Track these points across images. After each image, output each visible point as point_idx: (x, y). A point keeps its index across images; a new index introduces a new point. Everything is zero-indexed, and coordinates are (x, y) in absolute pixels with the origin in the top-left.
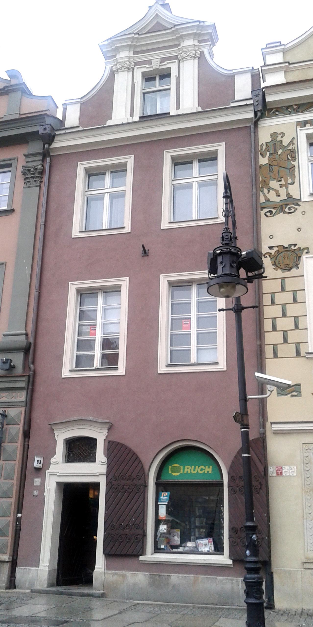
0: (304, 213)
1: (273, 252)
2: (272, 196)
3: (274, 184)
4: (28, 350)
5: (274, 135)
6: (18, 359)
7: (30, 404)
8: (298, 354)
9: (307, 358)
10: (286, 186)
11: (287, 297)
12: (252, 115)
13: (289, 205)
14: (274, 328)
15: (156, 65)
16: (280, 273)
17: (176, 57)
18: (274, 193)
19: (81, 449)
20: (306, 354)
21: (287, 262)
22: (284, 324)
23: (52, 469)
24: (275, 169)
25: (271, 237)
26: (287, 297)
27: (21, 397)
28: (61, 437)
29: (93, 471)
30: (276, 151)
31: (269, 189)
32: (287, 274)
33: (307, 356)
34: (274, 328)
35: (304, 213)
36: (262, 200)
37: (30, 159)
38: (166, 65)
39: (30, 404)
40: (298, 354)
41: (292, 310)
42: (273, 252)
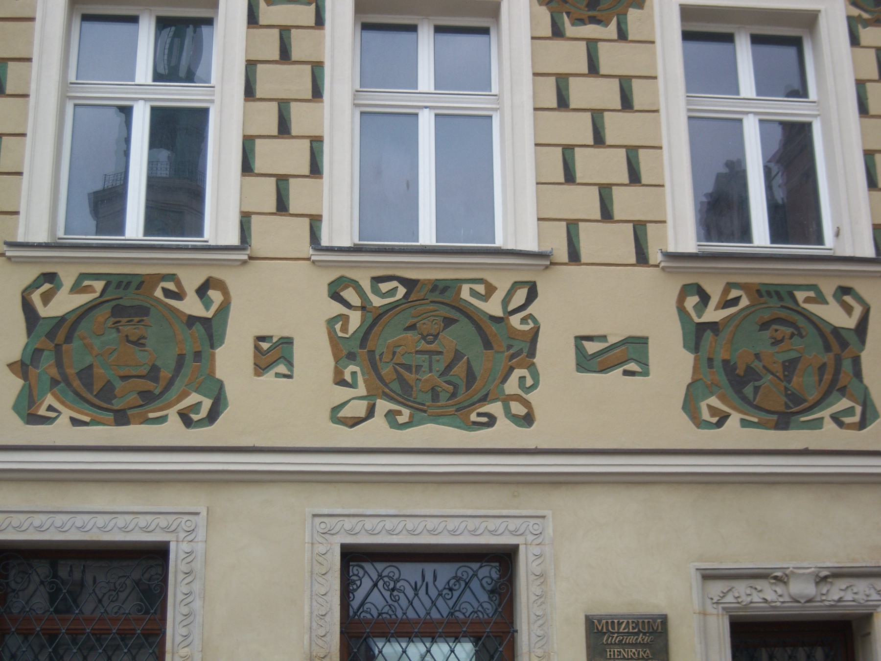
9: (9, 258)
20: (5, 248)
33: (8, 254)
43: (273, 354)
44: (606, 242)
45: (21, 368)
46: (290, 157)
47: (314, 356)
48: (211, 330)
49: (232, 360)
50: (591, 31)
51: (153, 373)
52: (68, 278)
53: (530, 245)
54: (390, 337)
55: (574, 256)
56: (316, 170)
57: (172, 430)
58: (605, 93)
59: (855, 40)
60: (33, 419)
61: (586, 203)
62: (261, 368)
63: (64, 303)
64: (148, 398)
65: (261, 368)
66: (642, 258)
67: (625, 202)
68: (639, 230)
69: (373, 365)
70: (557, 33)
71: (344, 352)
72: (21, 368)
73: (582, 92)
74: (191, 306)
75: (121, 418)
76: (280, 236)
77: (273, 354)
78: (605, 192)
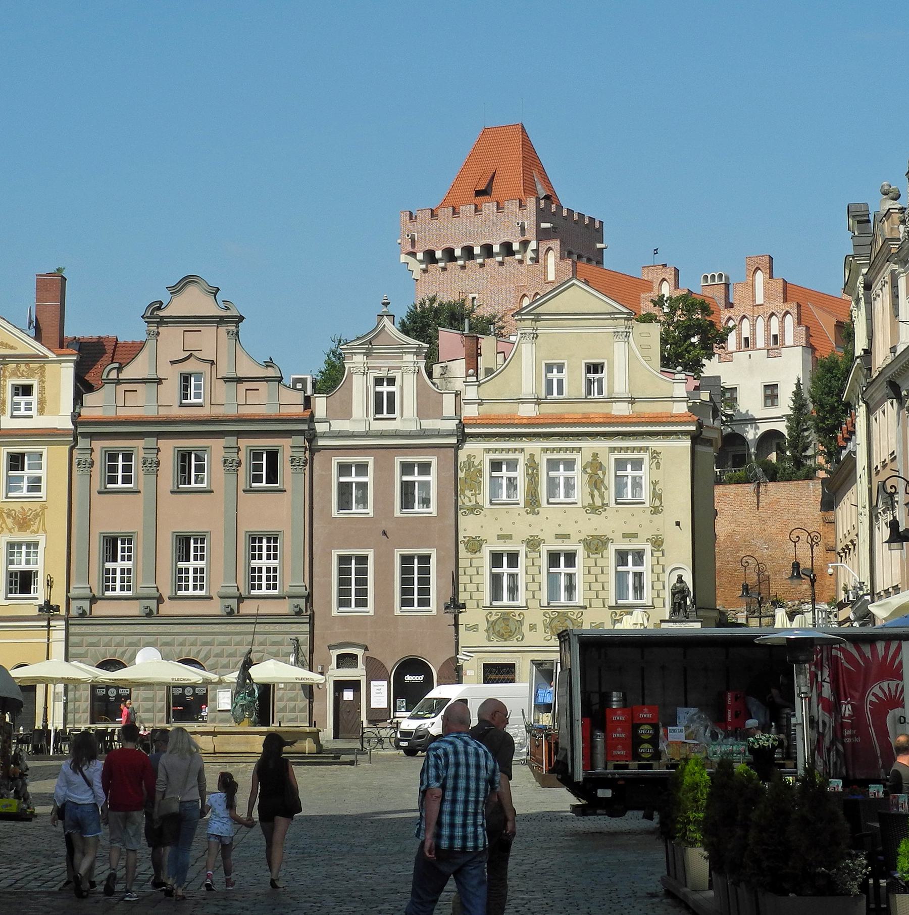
0: (485, 516)
1: (466, 540)
2: (466, 501)
3: (467, 493)
4: (309, 598)
5: (469, 456)
6: (302, 602)
7: (312, 633)
8: (478, 606)
10: (475, 495)
11: (472, 571)
12: (455, 441)
13: (476, 509)
14: (465, 590)
15: (383, 373)
16: (470, 555)
17: (400, 368)
18: (467, 499)
19: (346, 660)
21: (473, 547)
22: (471, 587)
23: (330, 672)
24: (469, 481)
25: (465, 530)
26: (472, 571)
27: (306, 628)
28: (335, 653)
29: (358, 673)
30: (469, 468)
31: (465, 495)
32: (474, 556)
34: (465, 590)
35: (485, 516)
36: (460, 503)
37: (294, 450)
38: (391, 374)
39: (312, 633)
40: (478, 606)
41: (476, 579)
42: (466, 540)
43: (533, 627)
44: (597, 603)
45: (487, 631)
46: (535, 587)
47: (540, 627)
48: (521, 623)
49: (525, 628)
50: (596, 556)
51: (511, 631)
52: (494, 612)
53: (582, 604)
54: (555, 623)
55: (590, 606)
56: (540, 589)
57: (515, 643)
58: (598, 570)
59: (652, 555)
60: (490, 640)
61: (593, 594)
62: (531, 630)
63: (494, 618)
64: (510, 636)
65: (531, 630)
66: (604, 606)
67: (602, 594)
68: (604, 599)
69: (552, 629)
70: (589, 557)
71: (546, 627)
72: (487, 631)
73: (595, 570)
74: (517, 618)
75: (506, 640)
76: (533, 604)
77: (533, 627)
78: (597, 592)
